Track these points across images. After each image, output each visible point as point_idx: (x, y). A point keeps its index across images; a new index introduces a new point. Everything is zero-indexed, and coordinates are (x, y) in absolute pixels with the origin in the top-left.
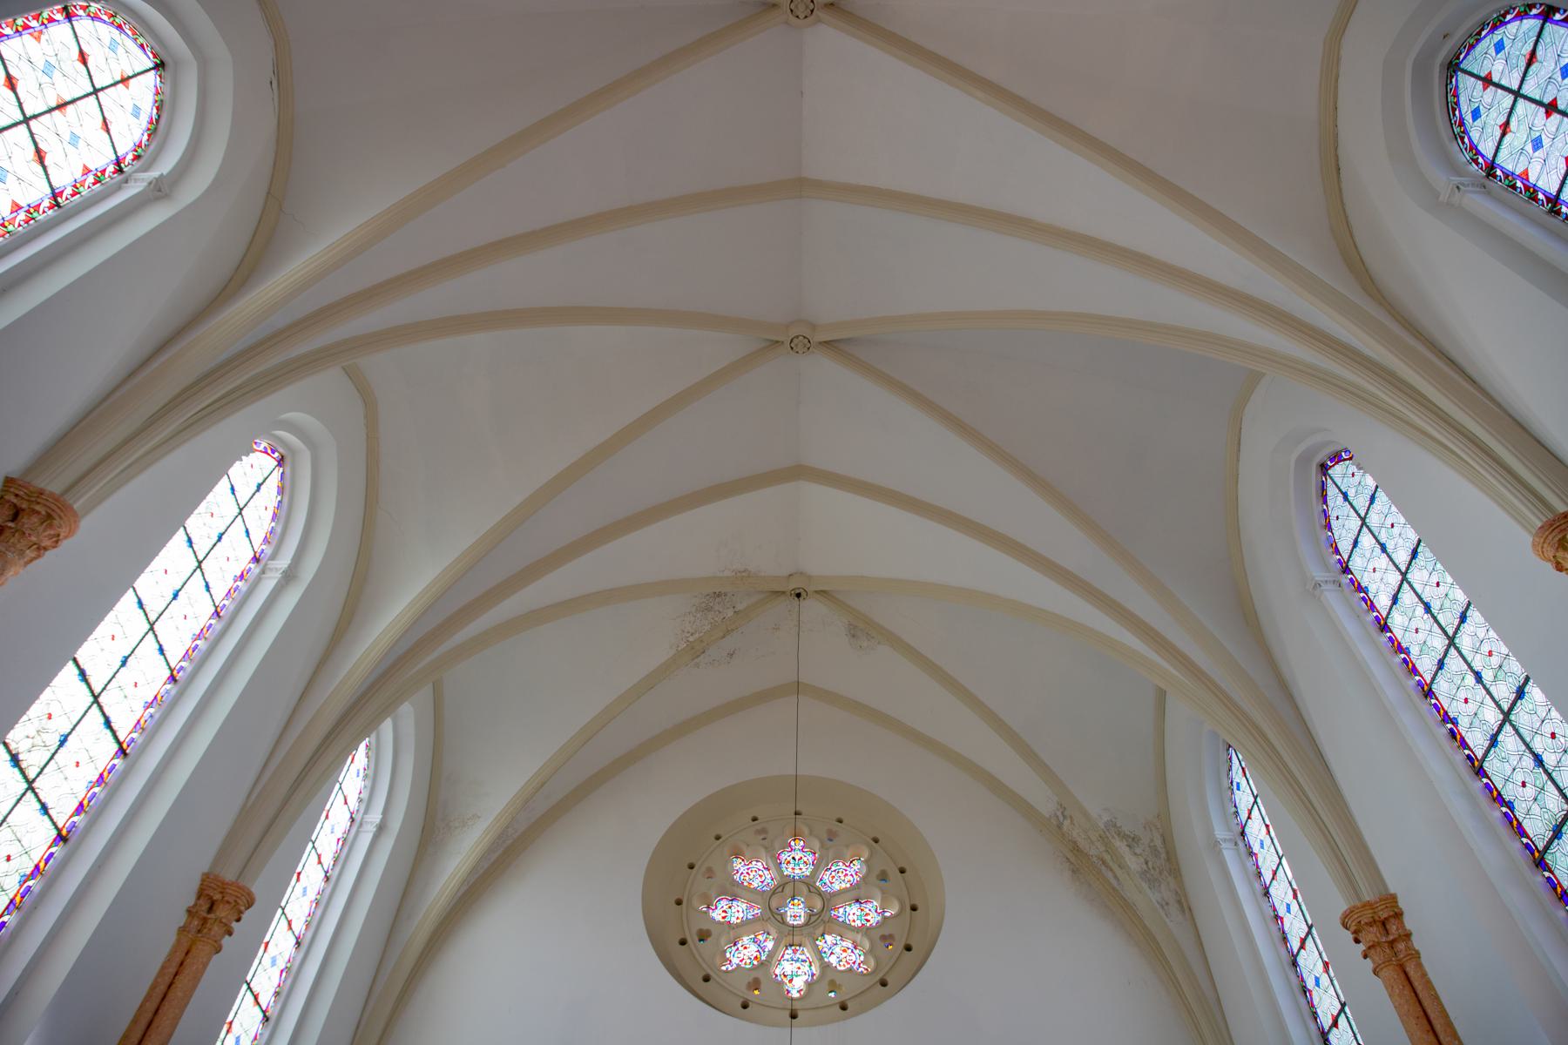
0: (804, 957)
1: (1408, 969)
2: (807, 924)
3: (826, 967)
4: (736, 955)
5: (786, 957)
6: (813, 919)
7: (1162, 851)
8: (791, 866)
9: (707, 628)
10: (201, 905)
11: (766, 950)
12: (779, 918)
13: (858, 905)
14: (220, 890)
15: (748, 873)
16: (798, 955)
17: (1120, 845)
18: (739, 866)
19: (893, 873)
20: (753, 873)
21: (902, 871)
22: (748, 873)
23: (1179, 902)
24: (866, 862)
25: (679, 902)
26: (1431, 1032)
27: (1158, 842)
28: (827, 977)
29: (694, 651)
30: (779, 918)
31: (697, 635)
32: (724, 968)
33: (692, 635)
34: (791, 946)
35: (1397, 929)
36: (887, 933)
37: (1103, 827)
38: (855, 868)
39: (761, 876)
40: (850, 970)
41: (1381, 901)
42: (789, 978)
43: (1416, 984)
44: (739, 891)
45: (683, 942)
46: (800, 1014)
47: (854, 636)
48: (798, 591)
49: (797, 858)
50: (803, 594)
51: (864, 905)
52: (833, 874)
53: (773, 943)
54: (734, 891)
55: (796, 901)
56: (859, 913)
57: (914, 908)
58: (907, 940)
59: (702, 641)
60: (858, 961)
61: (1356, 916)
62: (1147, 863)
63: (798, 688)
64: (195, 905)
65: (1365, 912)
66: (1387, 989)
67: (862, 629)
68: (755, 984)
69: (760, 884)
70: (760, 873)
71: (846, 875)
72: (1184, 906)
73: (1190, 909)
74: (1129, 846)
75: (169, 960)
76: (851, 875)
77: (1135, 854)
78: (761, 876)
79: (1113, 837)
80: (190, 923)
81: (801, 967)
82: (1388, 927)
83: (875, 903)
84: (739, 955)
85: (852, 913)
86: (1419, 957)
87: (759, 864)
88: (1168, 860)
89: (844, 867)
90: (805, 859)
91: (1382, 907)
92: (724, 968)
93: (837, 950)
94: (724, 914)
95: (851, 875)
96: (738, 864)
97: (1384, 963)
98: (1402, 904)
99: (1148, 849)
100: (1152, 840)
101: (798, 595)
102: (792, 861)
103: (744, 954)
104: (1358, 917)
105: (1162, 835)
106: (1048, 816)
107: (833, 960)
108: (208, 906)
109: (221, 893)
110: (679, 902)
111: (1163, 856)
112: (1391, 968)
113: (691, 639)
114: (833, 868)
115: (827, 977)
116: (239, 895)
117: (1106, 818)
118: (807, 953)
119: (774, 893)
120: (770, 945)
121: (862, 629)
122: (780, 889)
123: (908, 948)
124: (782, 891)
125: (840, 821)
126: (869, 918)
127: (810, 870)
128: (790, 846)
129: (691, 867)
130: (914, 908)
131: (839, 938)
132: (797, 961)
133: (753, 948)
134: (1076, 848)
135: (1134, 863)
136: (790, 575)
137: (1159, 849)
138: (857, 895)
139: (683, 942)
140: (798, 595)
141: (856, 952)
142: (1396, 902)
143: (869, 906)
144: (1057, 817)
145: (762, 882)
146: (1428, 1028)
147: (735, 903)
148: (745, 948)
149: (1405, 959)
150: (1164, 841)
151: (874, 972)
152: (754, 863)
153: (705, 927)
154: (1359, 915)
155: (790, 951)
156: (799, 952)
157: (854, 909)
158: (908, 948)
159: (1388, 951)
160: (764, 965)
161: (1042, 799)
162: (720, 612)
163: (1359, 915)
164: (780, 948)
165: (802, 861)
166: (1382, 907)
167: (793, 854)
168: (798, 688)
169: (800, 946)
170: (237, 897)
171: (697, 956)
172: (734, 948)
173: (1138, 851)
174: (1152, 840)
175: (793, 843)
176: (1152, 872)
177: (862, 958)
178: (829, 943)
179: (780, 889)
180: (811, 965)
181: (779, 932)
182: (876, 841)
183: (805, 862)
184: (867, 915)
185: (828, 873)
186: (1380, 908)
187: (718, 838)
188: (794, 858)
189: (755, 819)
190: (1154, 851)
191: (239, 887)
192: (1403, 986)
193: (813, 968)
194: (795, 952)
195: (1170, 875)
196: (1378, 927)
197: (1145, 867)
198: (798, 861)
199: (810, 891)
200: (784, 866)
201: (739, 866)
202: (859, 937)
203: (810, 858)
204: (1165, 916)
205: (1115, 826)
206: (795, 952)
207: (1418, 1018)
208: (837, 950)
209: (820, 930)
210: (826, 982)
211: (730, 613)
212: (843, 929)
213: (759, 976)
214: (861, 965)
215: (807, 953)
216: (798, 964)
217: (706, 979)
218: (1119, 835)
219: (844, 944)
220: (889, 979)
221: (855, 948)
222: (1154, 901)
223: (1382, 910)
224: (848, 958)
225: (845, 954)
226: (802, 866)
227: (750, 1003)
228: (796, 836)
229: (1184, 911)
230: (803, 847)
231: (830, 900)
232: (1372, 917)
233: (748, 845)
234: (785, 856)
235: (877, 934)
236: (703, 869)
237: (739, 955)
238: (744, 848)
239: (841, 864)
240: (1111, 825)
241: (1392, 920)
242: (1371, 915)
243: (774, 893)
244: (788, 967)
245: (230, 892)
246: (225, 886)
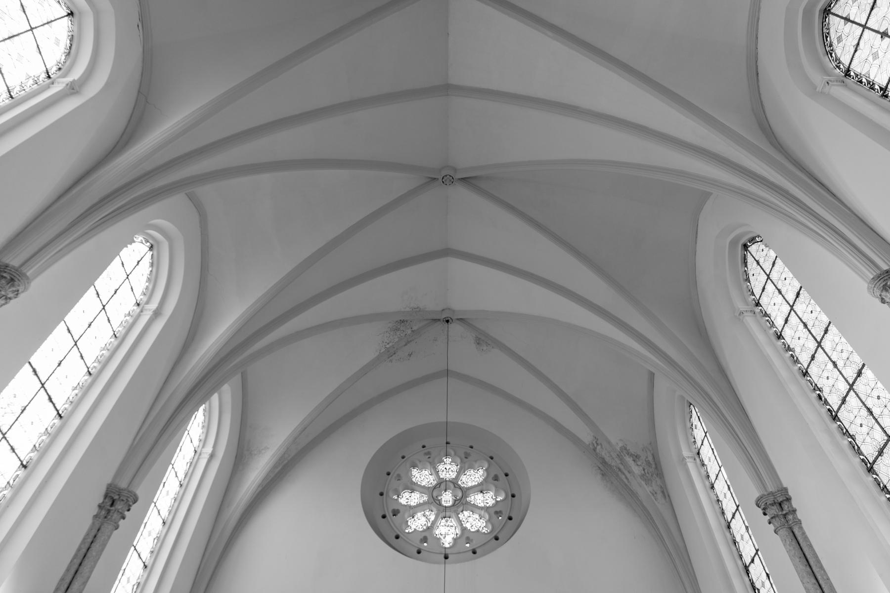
0: (451, 524)
1: (794, 530)
2: (453, 505)
3: (464, 529)
4: (414, 523)
5: (442, 524)
6: (457, 502)
8: (445, 472)
9: (396, 340)
10: (106, 503)
11: (431, 520)
12: (438, 502)
13: (482, 494)
14: (117, 493)
15: (420, 477)
16: (448, 523)
17: (629, 460)
18: (415, 473)
19: (502, 476)
20: (423, 477)
21: (507, 475)
22: (420, 477)
23: (663, 492)
25: (382, 494)
26: (808, 566)
27: (650, 458)
28: (465, 535)
29: (389, 353)
30: (438, 502)
31: (391, 344)
33: (388, 344)
34: (445, 518)
35: (788, 507)
36: (498, 510)
37: (619, 449)
38: (480, 473)
39: (427, 479)
40: (478, 531)
41: (778, 491)
43: (799, 538)
44: (414, 487)
45: (384, 517)
47: (478, 344)
48: (447, 319)
49: (447, 468)
50: (450, 321)
51: (485, 494)
52: (468, 477)
54: (412, 487)
55: (447, 492)
56: (482, 499)
57: (513, 496)
58: (509, 514)
59: (394, 348)
60: (482, 526)
61: (764, 500)
63: (447, 373)
64: (103, 502)
65: (769, 498)
66: (782, 541)
67: (483, 340)
68: (425, 540)
69: (427, 483)
70: (427, 477)
71: (475, 477)
72: (665, 493)
73: (669, 496)
74: (634, 461)
75: (88, 534)
76: (478, 478)
77: (638, 465)
78: (427, 479)
79: (625, 456)
80: (100, 512)
81: (450, 530)
82: (783, 506)
83: (491, 493)
84: (415, 524)
85: (478, 499)
86: (801, 523)
87: (426, 472)
88: (656, 468)
89: (474, 473)
90: (452, 469)
91: (780, 495)
92: (407, 531)
93: (470, 519)
94: (407, 501)
95: (478, 478)
96: (415, 472)
97: (780, 526)
98: (791, 493)
99: (645, 462)
100: (647, 457)
101: (448, 321)
102: (445, 470)
103: (417, 523)
104: (765, 501)
105: (653, 455)
106: (588, 443)
107: (468, 526)
108: (110, 503)
109: (119, 495)
110: (382, 494)
111: (654, 466)
112: (784, 529)
113: (388, 346)
114: (468, 474)
115: (465, 535)
116: (129, 496)
117: (620, 445)
118: (453, 522)
120: (432, 518)
121: (483, 340)
122: (438, 486)
123: (510, 518)
124: (440, 487)
125: (472, 447)
126: (488, 501)
128: (444, 461)
129: (388, 474)
130: (513, 496)
131: (471, 513)
133: (424, 519)
134: (604, 462)
135: (637, 470)
136: (443, 310)
137: (651, 462)
138: (481, 488)
139: (384, 517)
140: (448, 321)
142: (787, 492)
144: (593, 444)
145: (428, 482)
146: (806, 563)
147: (413, 494)
148: (419, 519)
149: (793, 524)
150: (654, 458)
151: (491, 532)
152: (424, 471)
153: (396, 508)
154: (766, 499)
155: (444, 521)
156: (449, 521)
158: (510, 518)
159: (783, 520)
160: (430, 529)
161: (586, 436)
162: (403, 331)
163: (766, 499)
164: (439, 519)
165: (450, 470)
166: (780, 495)
167: (445, 466)
168: (447, 373)
169: (450, 517)
170: (128, 497)
171: (391, 522)
172: (413, 520)
173: (639, 463)
174: (647, 457)
175: (445, 460)
176: (647, 475)
177: (484, 524)
178: (466, 516)
179: (438, 486)
180: (456, 529)
181: (438, 510)
182: (492, 458)
183: (452, 471)
184: (487, 500)
185: (465, 476)
186: (778, 495)
187: (403, 457)
188: (446, 468)
189: (424, 447)
190: (648, 463)
191: (129, 492)
192: (792, 540)
193: (457, 530)
194: (447, 521)
195: (657, 476)
196: (776, 506)
197: (643, 472)
198: (448, 469)
199: (455, 487)
200: (440, 473)
201: (415, 473)
202: (482, 512)
204: (655, 500)
205: (626, 449)
206: (447, 521)
207: (800, 558)
209: (461, 509)
210: (464, 538)
211: (409, 332)
212: (474, 508)
213: (427, 535)
214: (484, 528)
216: (449, 528)
217: (397, 537)
218: (628, 454)
219: (474, 516)
221: (481, 519)
222: (649, 492)
223: (779, 496)
224: (476, 524)
225: (474, 522)
226: (450, 473)
227: (422, 551)
228: (447, 455)
230: (451, 462)
231: (466, 492)
232: (774, 501)
233: (420, 461)
235: (492, 511)
236: (395, 475)
237: (415, 524)
238: (417, 462)
240: (624, 448)
241: (785, 502)
242: (772, 500)
245: (124, 494)
246: (121, 491)
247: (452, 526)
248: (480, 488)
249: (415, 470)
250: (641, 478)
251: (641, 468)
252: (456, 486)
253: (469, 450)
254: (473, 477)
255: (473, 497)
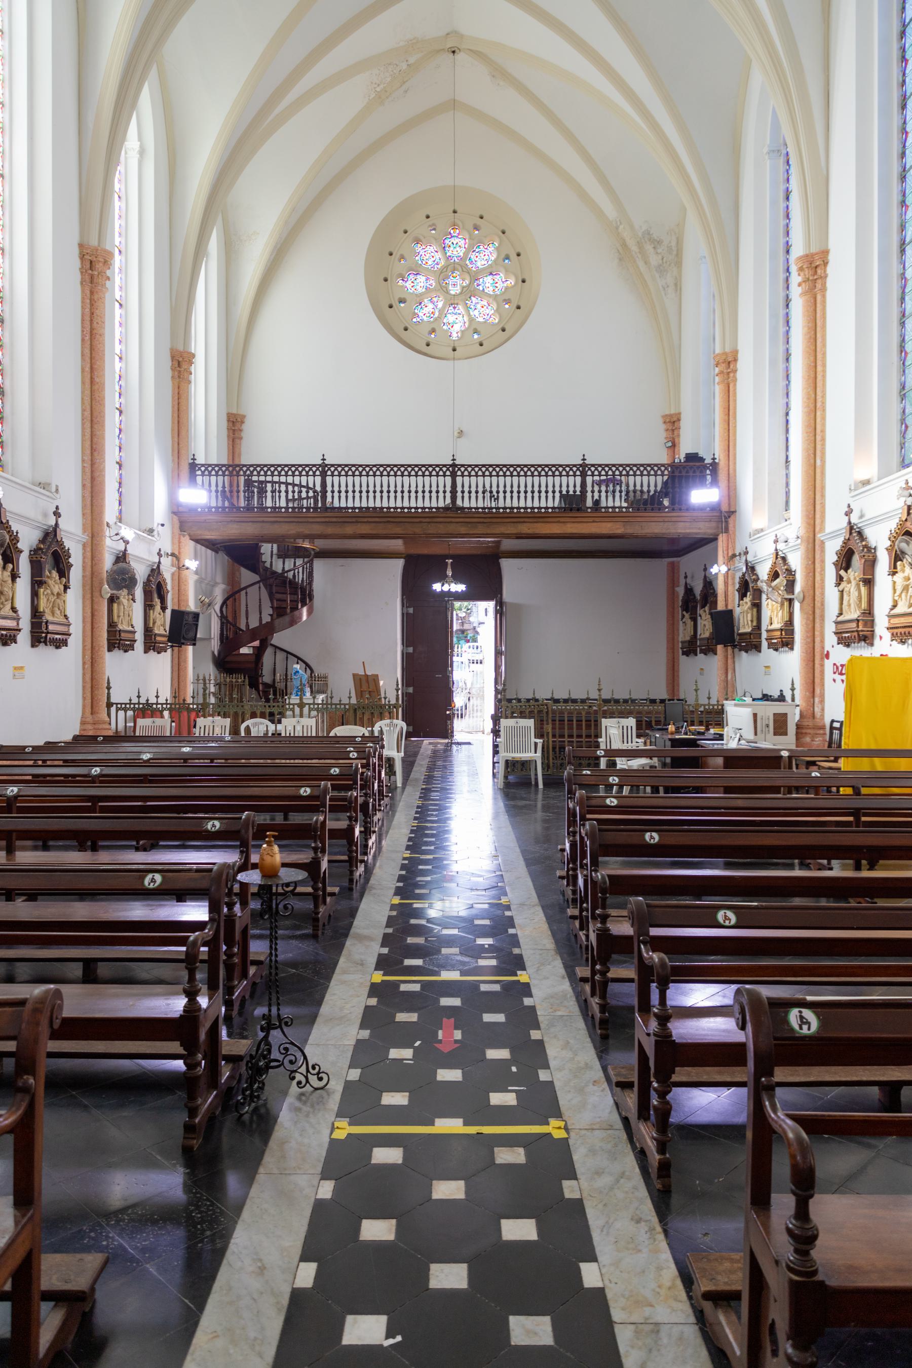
0: (459, 312)
2: (461, 293)
3: (472, 320)
5: (450, 311)
6: (465, 289)
7: (674, 249)
8: (452, 248)
13: (491, 276)
16: (456, 311)
17: (649, 248)
19: (513, 256)
21: (518, 255)
23: (676, 285)
24: (497, 249)
25: (386, 280)
27: (674, 244)
32: (414, 320)
42: (451, 325)
43: (731, 393)
45: (391, 307)
46: (458, 349)
47: (493, 76)
48: (453, 49)
49: (455, 243)
52: (477, 254)
53: (442, 302)
55: (455, 274)
56: (492, 281)
57: (524, 281)
62: (663, 259)
67: (499, 73)
70: (432, 254)
72: (678, 286)
74: (654, 248)
77: (657, 253)
79: (646, 242)
83: (501, 275)
85: (487, 283)
88: (677, 255)
90: (460, 244)
92: (414, 320)
96: (419, 248)
100: (670, 242)
102: (452, 245)
103: (426, 312)
105: (678, 239)
107: (476, 313)
110: (386, 280)
111: (675, 253)
114: (477, 250)
119: (441, 273)
120: (440, 305)
121: (499, 73)
122: (445, 270)
123: (518, 307)
125: (482, 217)
127: (463, 252)
128: (450, 233)
130: (524, 281)
132: (455, 314)
133: (431, 306)
134: (624, 245)
135: (654, 260)
136: (447, 34)
137: (673, 248)
139: (391, 307)
141: (489, 307)
143: (498, 277)
147: (418, 276)
150: (678, 243)
151: (499, 322)
153: (402, 296)
155: (451, 308)
157: (489, 279)
158: (518, 307)
162: (397, 65)
165: (458, 246)
167: (453, 240)
168: (453, 105)
173: (659, 251)
174: (670, 242)
175: (452, 232)
177: (493, 311)
179: (445, 270)
182: (504, 232)
185: (474, 253)
187: (406, 232)
189: (428, 217)
190: (670, 249)
194: (454, 308)
197: (661, 262)
200: (447, 249)
202: (491, 300)
203: (462, 242)
205: (649, 234)
206: (454, 308)
208: (479, 306)
209: (469, 295)
210: (472, 329)
211: (404, 66)
215: (461, 308)
216: (456, 316)
217: (406, 329)
219: (482, 302)
220: (507, 328)
225: (483, 309)
226: (458, 249)
228: (454, 226)
229: (677, 290)
230: (459, 234)
234: (447, 241)
236: (398, 256)
238: (422, 238)
239: (481, 247)
240: (648, 233)
243: (441, 273)
244: (450, 318)
247: (460, 314)
248: (489, 271)
249: (419, 245)
250: (656, 270)
251: (660, 257)
252: (464, 270)
253: (479, 222)
254: (484, 258)
255: (481, 280)
